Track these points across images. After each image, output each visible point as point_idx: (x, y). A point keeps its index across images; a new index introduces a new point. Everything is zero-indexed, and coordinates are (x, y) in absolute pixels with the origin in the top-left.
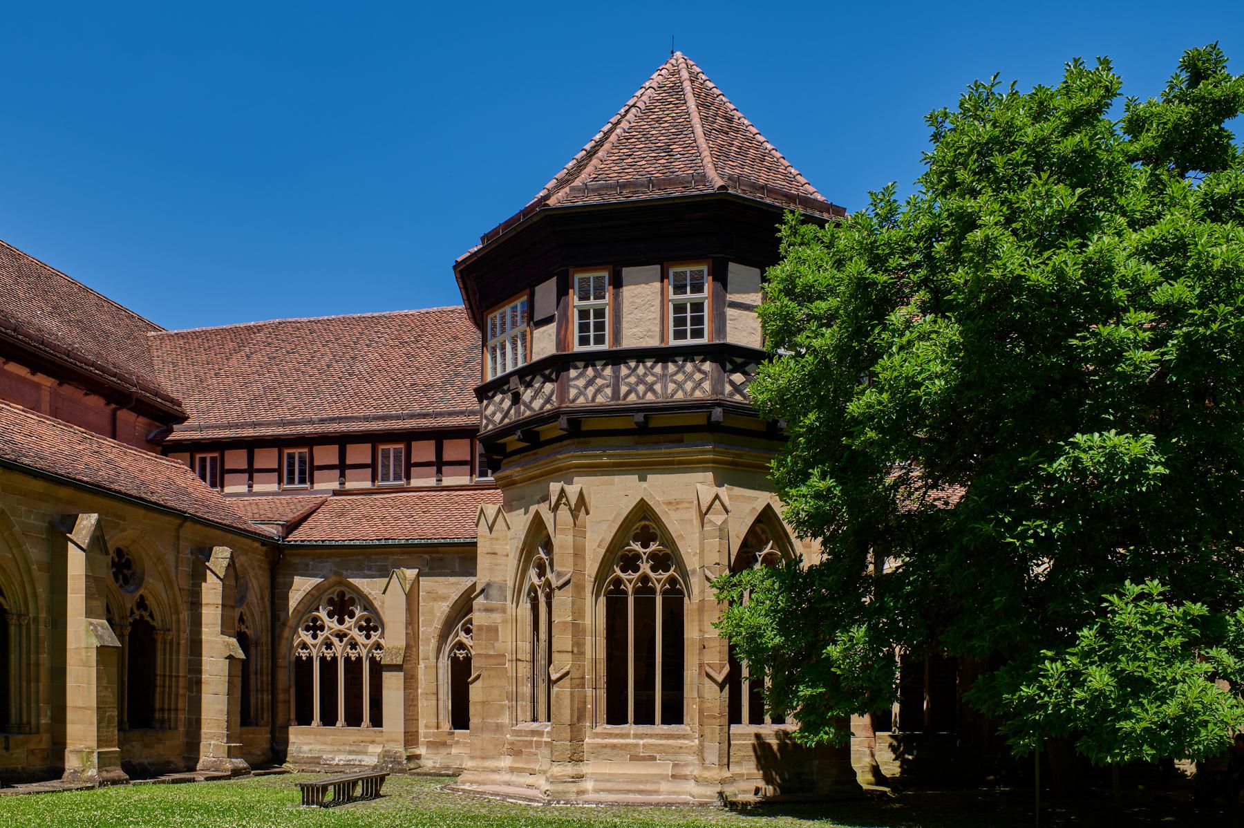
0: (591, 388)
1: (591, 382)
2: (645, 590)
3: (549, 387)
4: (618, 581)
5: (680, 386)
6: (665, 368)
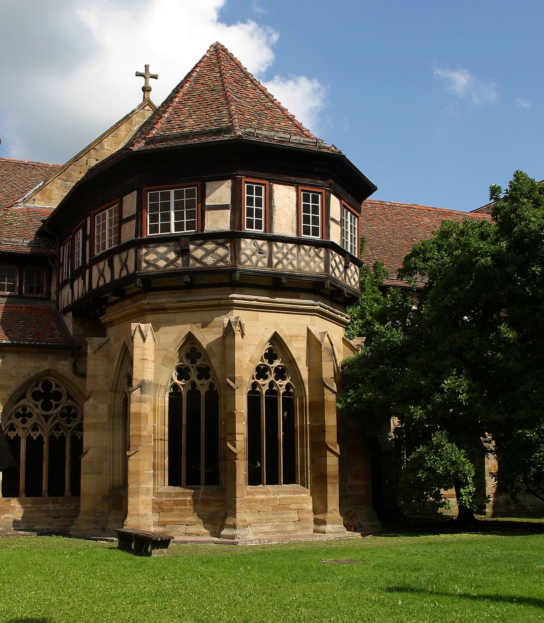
0: (254, 256)
3: (221, 251)
5: (308, 264)
6: (299, 250)
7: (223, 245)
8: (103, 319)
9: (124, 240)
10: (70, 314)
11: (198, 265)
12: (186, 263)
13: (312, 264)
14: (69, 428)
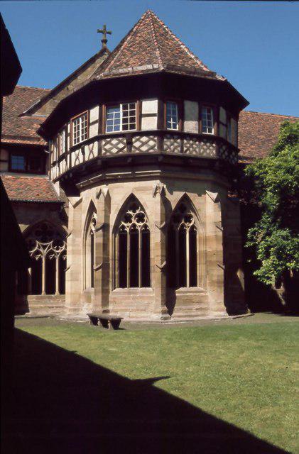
1: (172, 144)
2: (183, 232)
3: (152, 143)
4: (123, 227)
5: (205, 150)
7: (152, 139)
8: (80, 184)
9: (91, 136)
10: (58, 182)
11: (137, 151)
12: (130, 150)
13: (208, 151)
14: (58, 253)
